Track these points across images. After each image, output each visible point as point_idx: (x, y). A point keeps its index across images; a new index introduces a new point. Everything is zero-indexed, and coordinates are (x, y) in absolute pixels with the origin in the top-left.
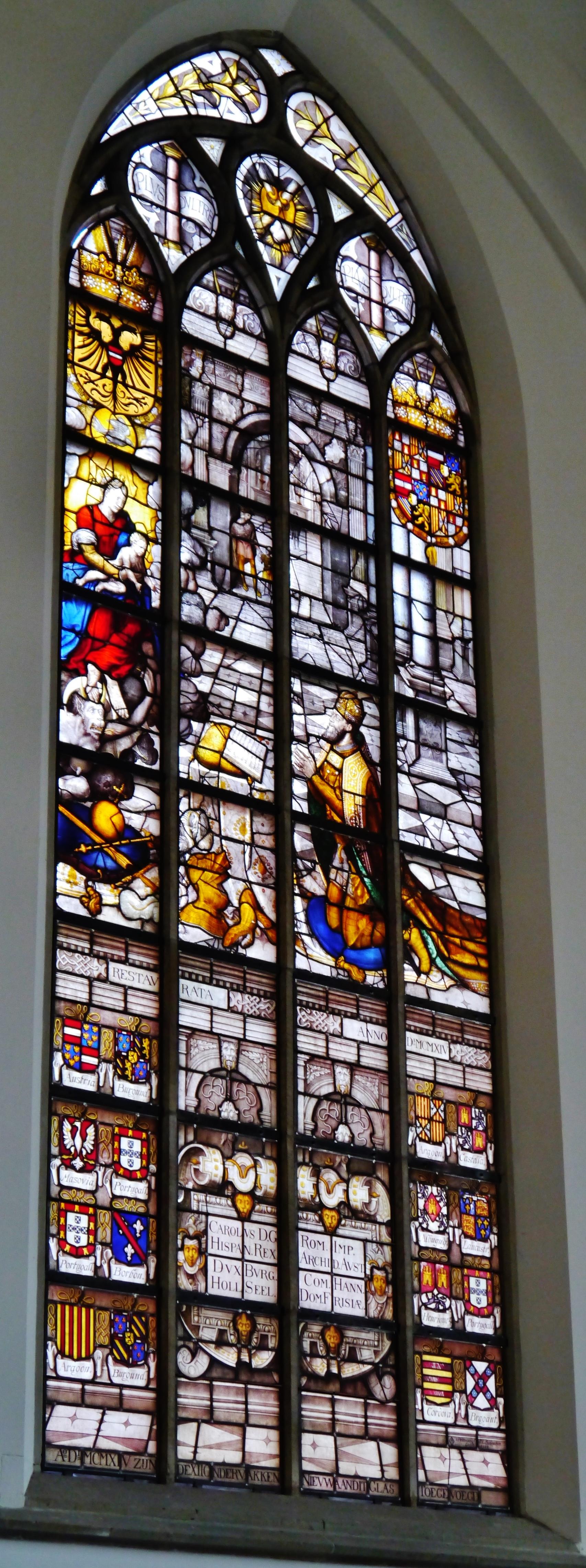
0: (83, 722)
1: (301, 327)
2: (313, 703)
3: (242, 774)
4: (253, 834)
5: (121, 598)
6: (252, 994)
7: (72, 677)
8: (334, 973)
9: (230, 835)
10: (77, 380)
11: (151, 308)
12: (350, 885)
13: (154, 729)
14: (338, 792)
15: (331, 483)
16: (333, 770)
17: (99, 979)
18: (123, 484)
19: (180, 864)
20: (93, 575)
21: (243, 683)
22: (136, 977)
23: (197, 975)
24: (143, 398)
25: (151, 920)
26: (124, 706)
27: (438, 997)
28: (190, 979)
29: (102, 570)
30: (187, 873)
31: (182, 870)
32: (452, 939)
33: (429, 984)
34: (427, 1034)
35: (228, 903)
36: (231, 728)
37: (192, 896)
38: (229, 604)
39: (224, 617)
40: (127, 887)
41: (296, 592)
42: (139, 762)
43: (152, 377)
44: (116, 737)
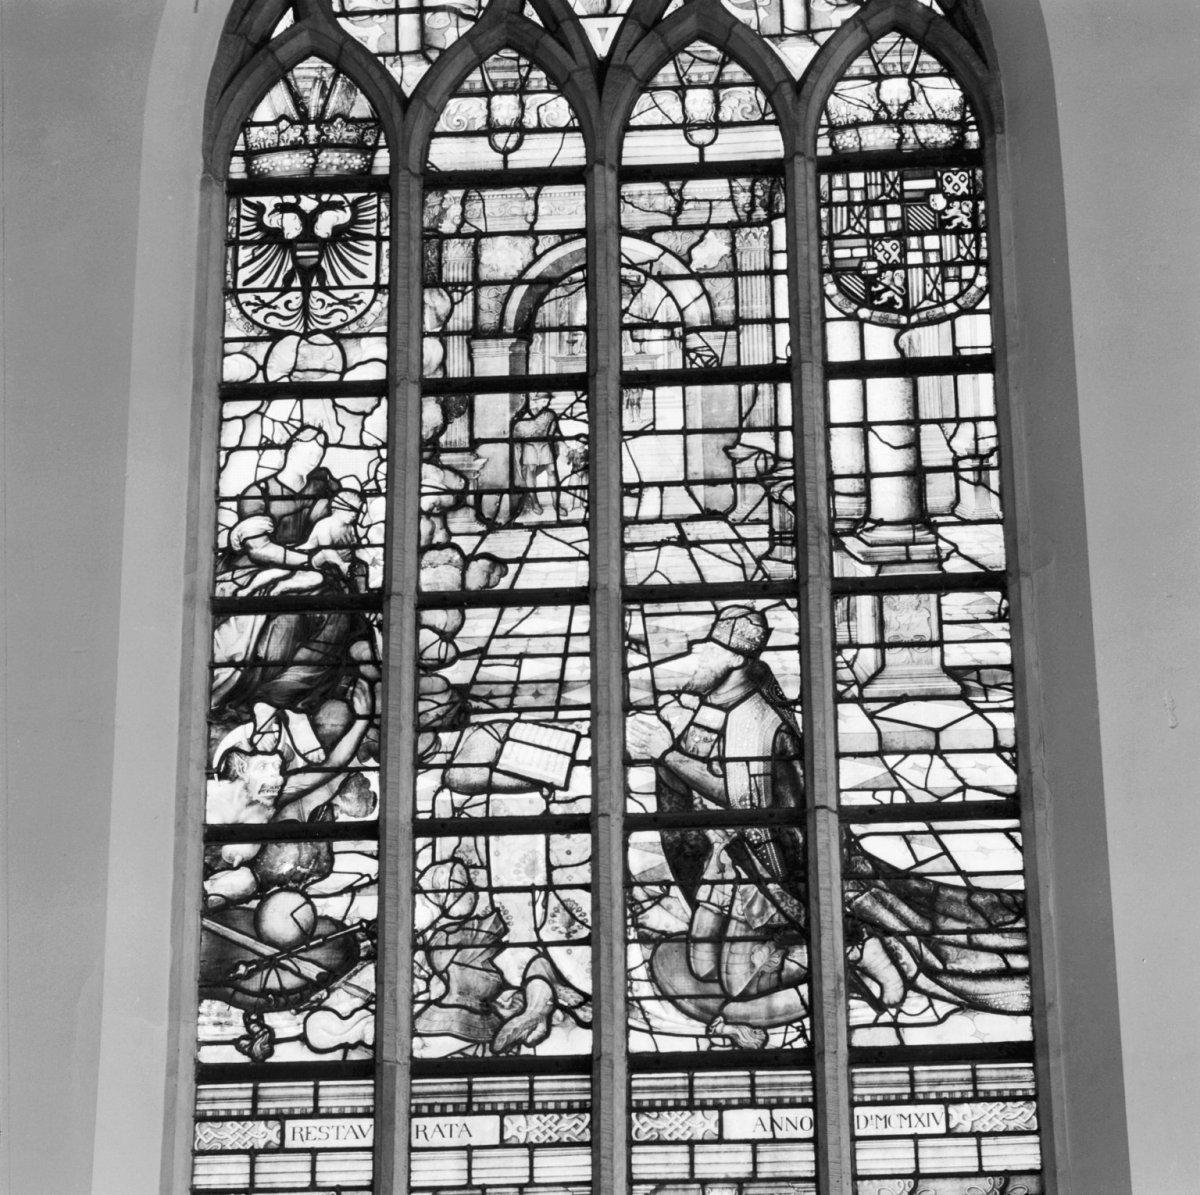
0: (246, 788)
1: (646, 86)
2: (666, 642)
3: (535, 785)
4: (550, 868)
5: (315, 593)
6: (545, 1112)
7: (228, 730)
8: (704, 1045)
9: (506, 883)
10: (242, 312)
11: (370, 164)
12: (737, 903)
13: (371, 763)
14: (716, 766)
15: (704, 299)
16: (706, 734)
17: (267, 1150)
18: (320, 430)
19: (415, 948)
20: (265, 577)
21: (532, 651)
22: (333, 1133)
23: (443, 1105)
24: (356, 296)
25: (361, 1043)
26: (317, 744)
27: (914, 1038)
28: (431, 1114)
29: (283, 566)
30: (429, 960)
31: (420, 956)
32: (950, 938)
33: (902, 1019)
34: (899, 1102)
35: (504, 985)
36: (511, 723)
37: (438, 987)
38: (508, 544)
39: (498, 563)
40: (320, 1006)
41: (632, 486)
42: (342, 818)
43: (372, 260)
44: (303, 793)
